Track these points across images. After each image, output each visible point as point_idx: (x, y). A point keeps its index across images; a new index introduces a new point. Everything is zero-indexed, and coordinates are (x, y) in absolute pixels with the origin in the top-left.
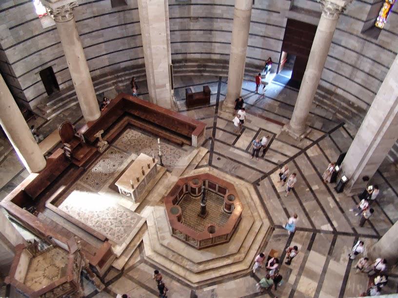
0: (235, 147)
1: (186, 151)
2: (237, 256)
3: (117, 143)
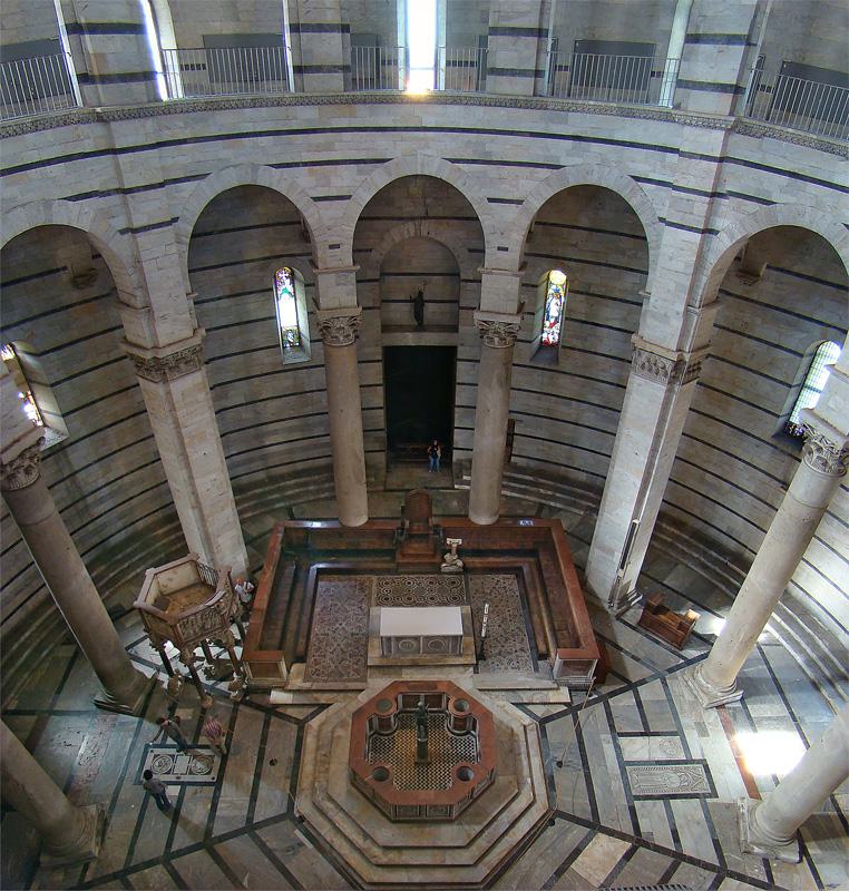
0: (614, 740)
1: (536, 669)
2: (377, 851)
3: (476, 581)
